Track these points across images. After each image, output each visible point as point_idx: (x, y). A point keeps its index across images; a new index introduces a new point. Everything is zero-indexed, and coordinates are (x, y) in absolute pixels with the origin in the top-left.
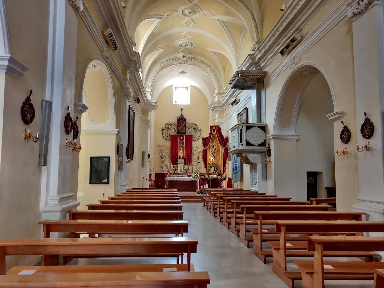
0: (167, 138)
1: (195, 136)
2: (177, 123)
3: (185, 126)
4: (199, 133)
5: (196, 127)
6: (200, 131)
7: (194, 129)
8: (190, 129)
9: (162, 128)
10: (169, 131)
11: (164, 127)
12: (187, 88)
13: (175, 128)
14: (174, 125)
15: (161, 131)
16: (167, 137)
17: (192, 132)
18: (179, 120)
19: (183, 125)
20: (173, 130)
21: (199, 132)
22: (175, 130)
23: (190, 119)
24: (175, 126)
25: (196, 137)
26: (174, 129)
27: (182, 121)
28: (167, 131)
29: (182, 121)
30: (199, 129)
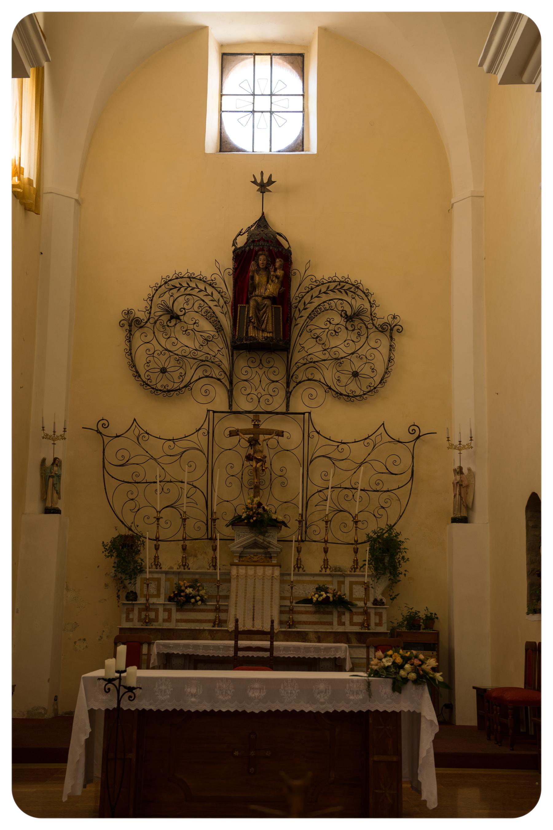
0: (161, 382)
1: (357, 365)
2: (230, 281)
3: (282, 300)
4: (384, 350)
5: (358, 303)
6: (391, 329)
7: (349, 318)
8: (320, 322)
9: (129, 312)
10: (177, 331)
11: (139, 306)
12: (297, 60)
13: (217, 310)
14: (210, 290)
15: (120, 335)
16: (163, 371)
17: (334, 342)
18: (243, 258)
19: (272, 289)
20: (206, 326)
21: (385, 341)
22: (219, 328)
23: (324, 245)
24: (216, 295)
25: (366, 370)
26: (211, 317)
27: (262, 259)
28: (160, 336)
29: (262, 259)
30: (383, 314)
